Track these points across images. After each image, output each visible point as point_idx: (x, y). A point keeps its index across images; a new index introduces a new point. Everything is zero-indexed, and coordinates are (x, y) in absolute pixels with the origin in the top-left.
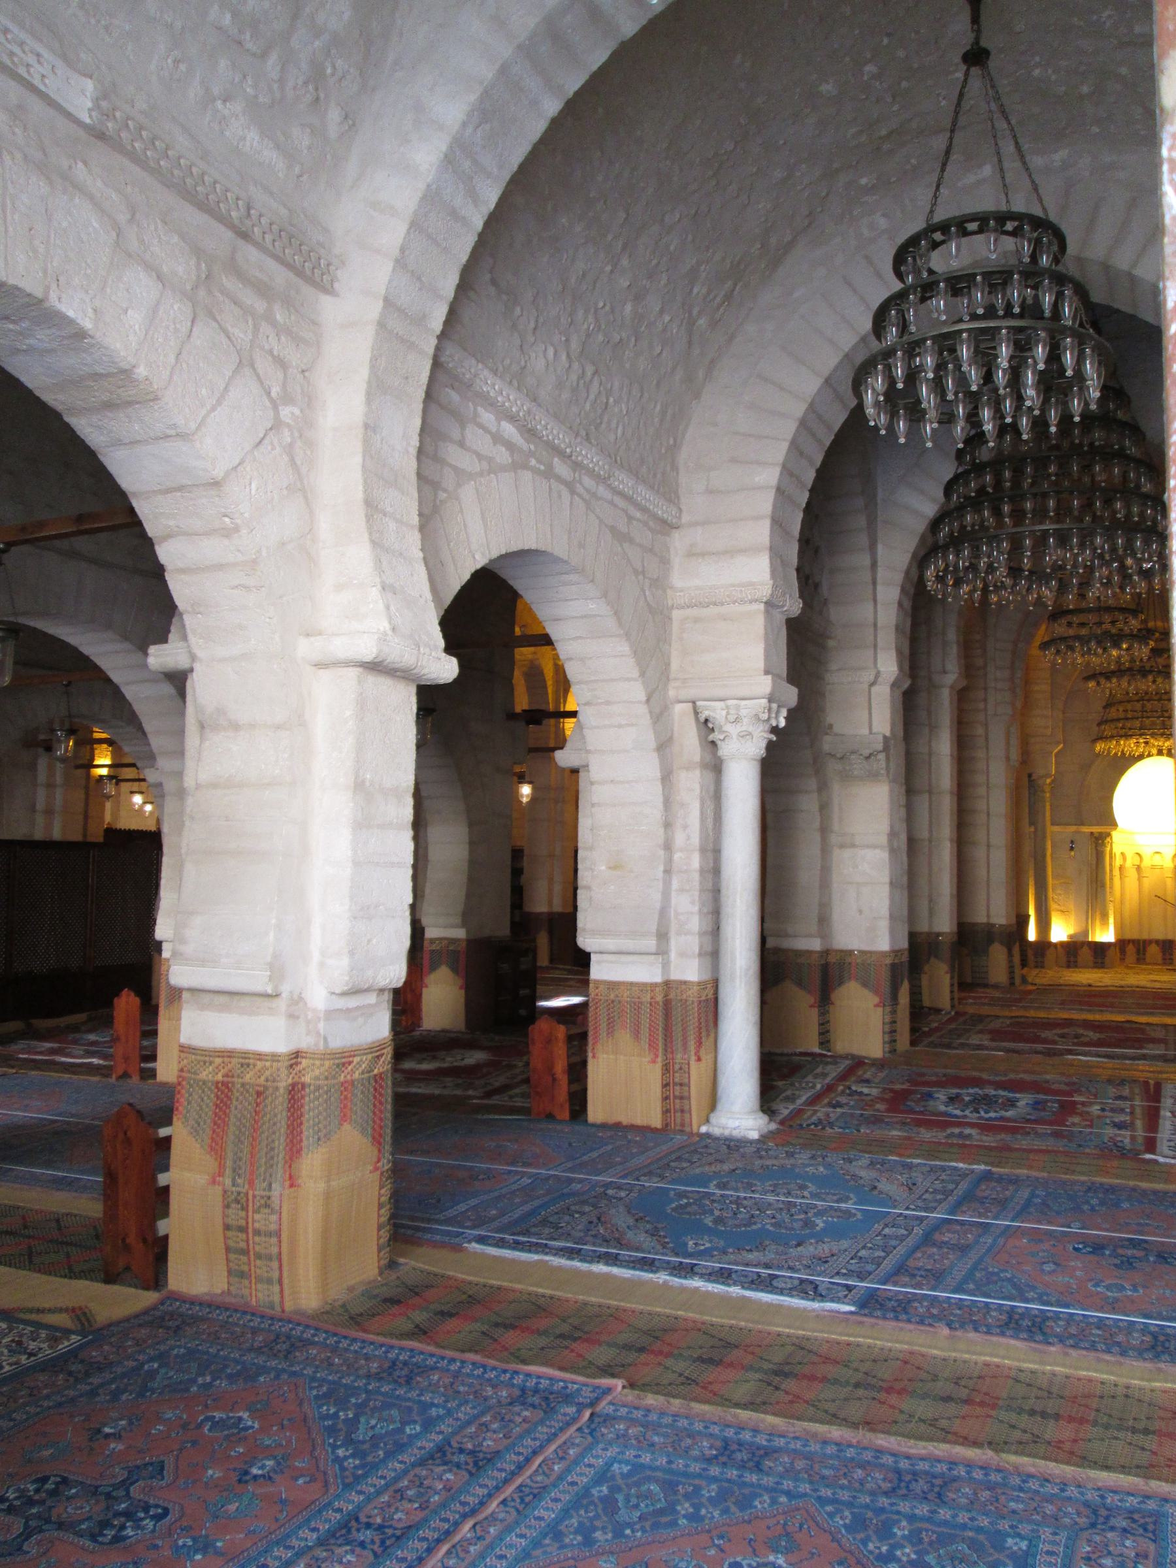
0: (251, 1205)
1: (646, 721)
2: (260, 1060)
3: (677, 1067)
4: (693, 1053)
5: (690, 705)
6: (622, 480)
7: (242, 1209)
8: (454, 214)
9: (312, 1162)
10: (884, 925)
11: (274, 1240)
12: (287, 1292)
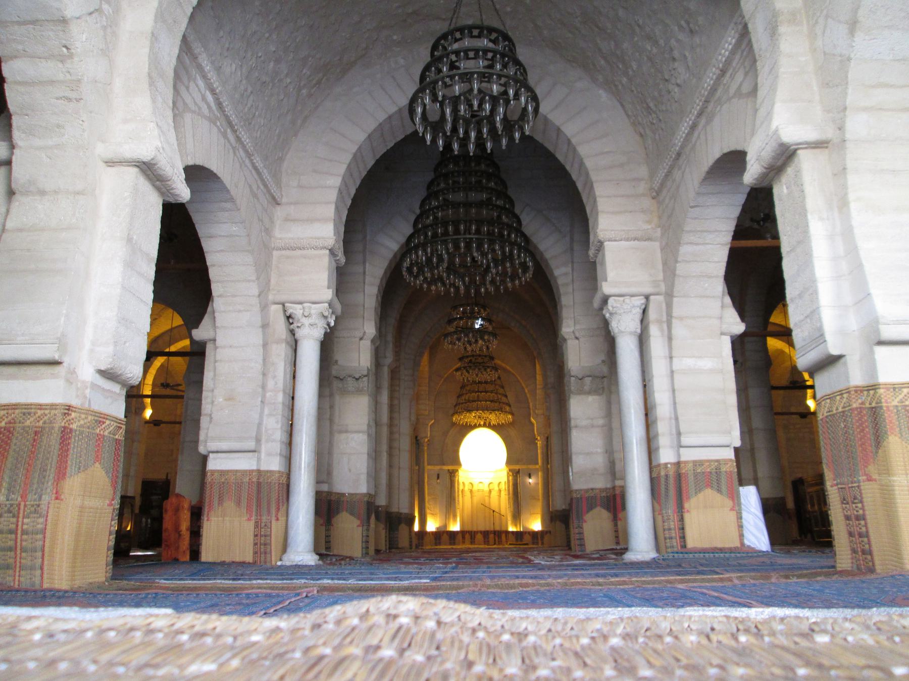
0: (21, 512)
1: (257, 309)
2: (41, 409)
3: (263, 524)
4: (274, 515)
5: (281, 306)
7: (14, 517)
9: (73, 484)
10: (364, 478)
11: (40, 536)
12: (45, 576)
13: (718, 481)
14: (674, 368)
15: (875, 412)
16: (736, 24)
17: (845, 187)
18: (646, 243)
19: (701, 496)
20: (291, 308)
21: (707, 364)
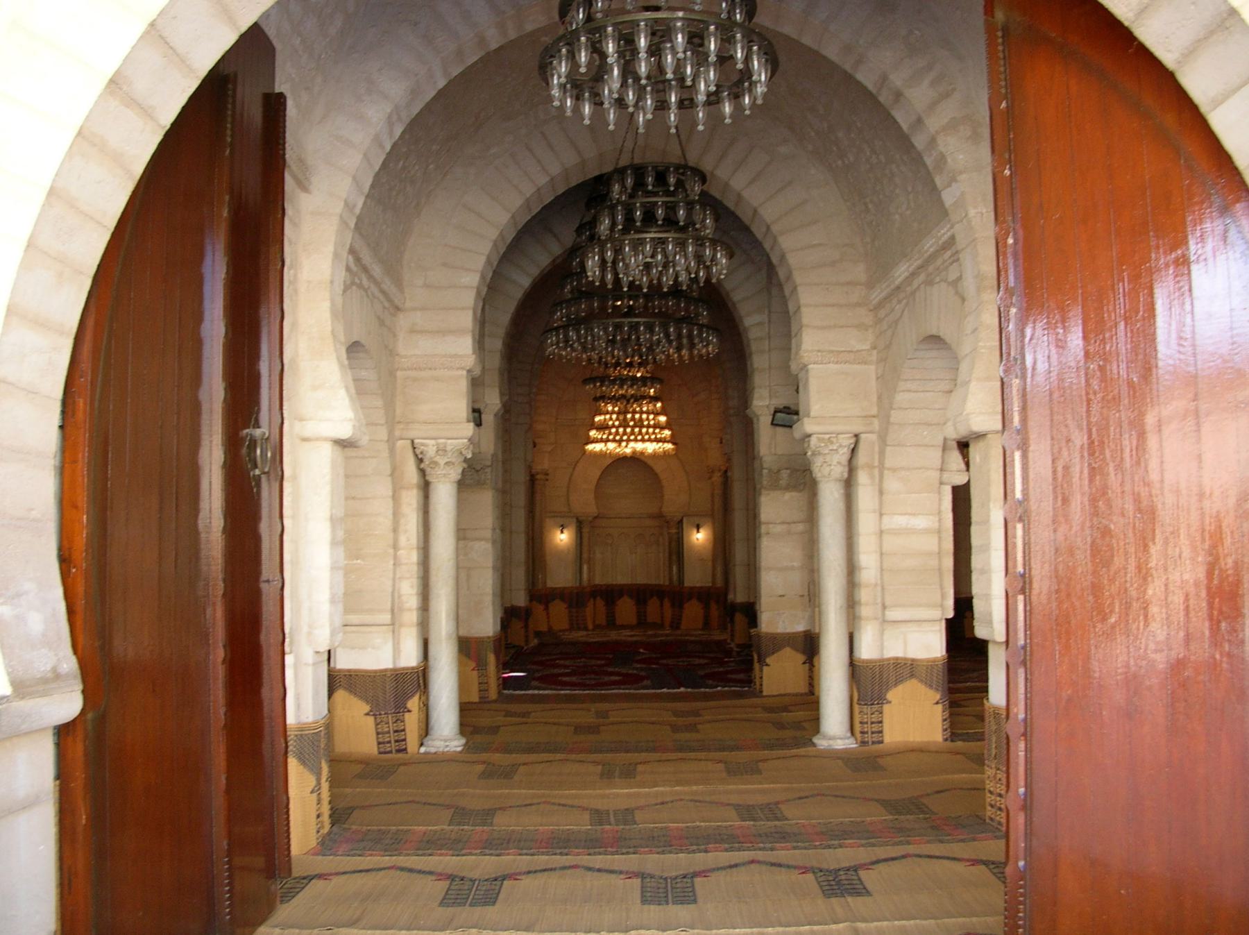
1: (386, 454)
6: (388, 285)
8: (382, 146)
20: (423, 445)
21: (921, 522)
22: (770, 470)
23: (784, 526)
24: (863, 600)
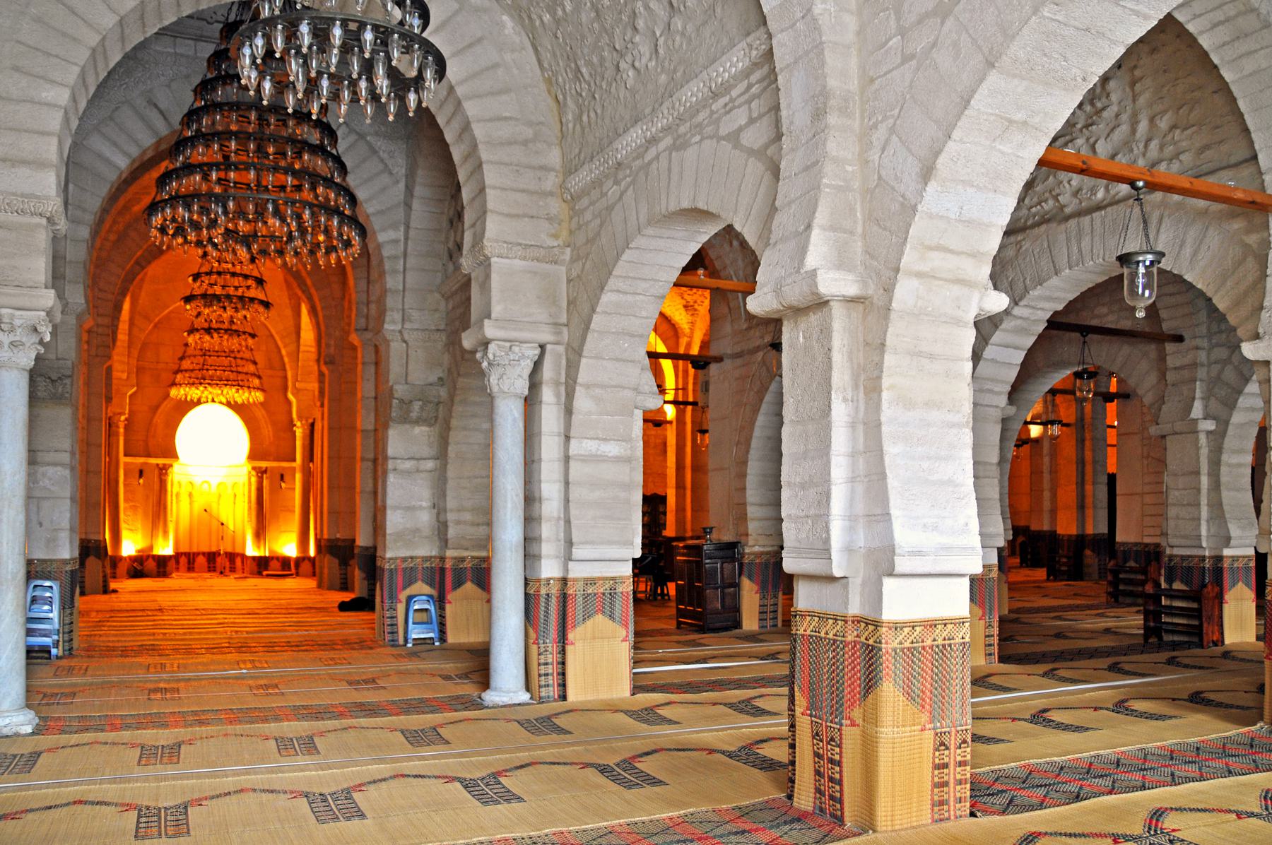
13: (612, 604)
14: (571, 453)
15: (871, 653)
16: (750, 46)
17: (879, 366)
18: (548, 266)
19: (589, 623)
21: (612, 449)
22: (402, 401)
23: (413, 463)
24: (544, 536)
